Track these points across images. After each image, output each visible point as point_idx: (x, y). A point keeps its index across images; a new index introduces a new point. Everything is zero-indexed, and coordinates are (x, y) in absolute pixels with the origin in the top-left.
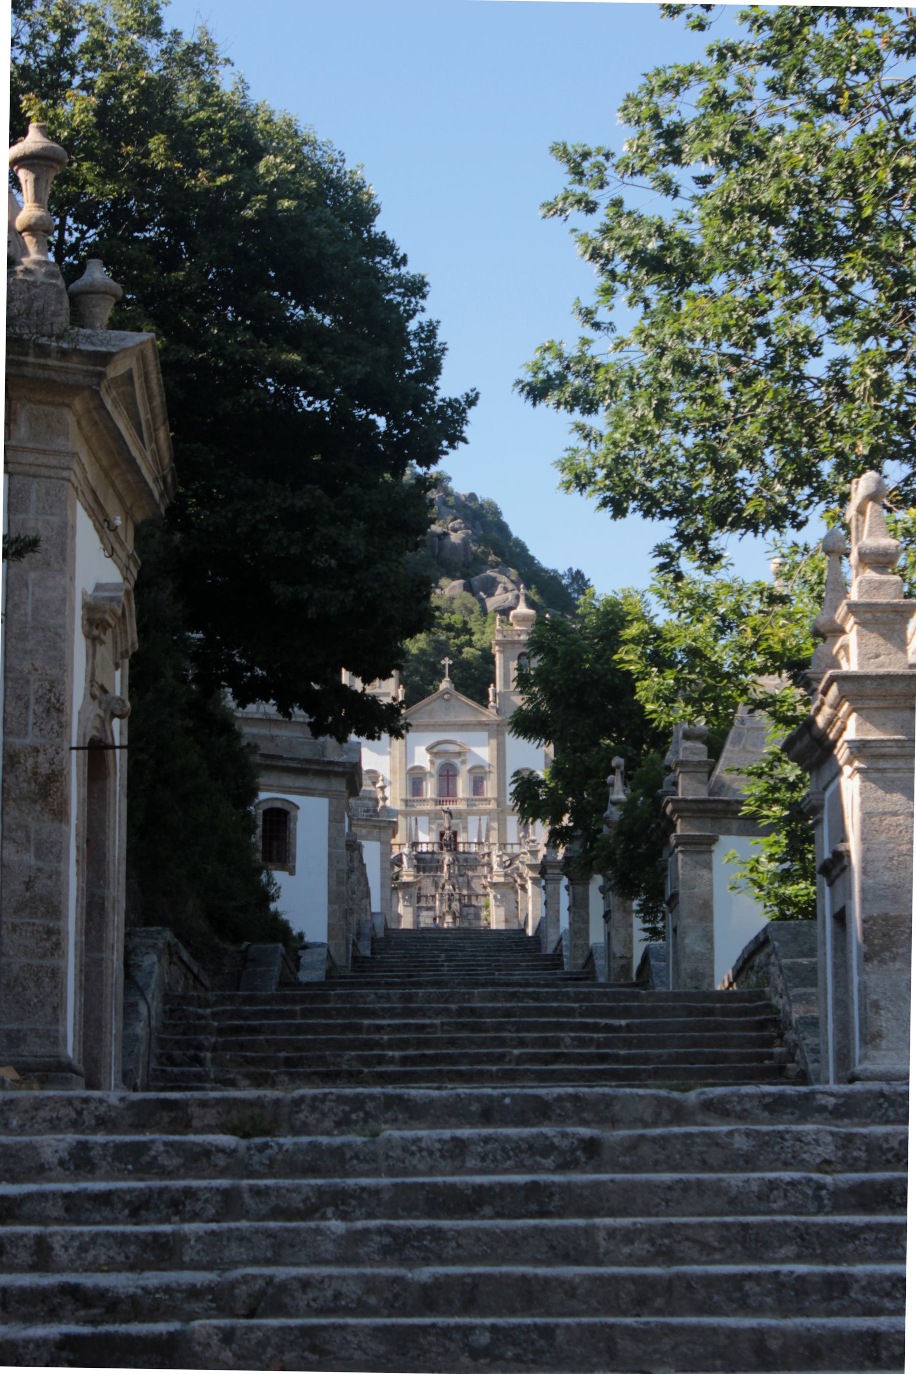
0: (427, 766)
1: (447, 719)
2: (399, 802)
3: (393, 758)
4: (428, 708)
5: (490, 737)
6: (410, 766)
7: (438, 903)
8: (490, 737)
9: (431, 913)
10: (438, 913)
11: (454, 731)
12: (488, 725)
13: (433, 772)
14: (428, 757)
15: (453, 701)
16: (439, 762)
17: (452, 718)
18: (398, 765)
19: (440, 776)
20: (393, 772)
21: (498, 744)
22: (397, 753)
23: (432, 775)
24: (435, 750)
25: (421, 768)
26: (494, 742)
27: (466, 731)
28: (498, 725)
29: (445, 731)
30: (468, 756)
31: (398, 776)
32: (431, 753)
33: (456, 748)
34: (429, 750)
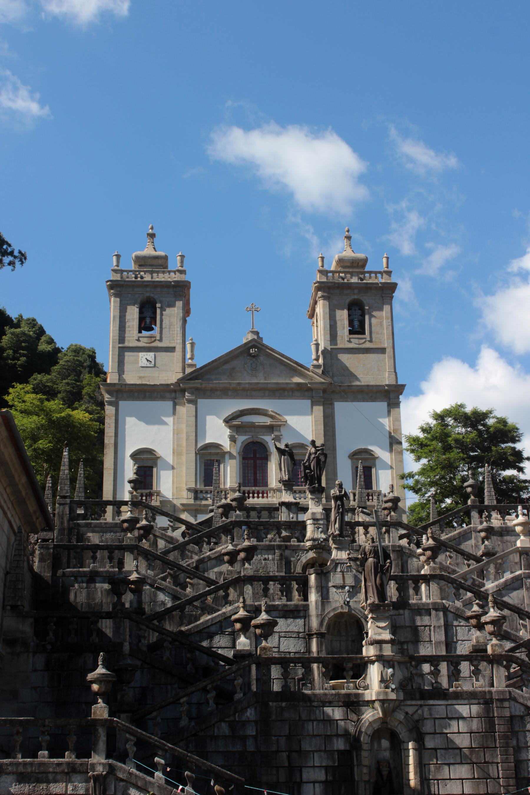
0: (226, 444)
1: (255, 381)
2: (185, 494)
3: (177, 433)
4: (227, 366)
5: (313, 404)
6: (200, 445)
7: (313, 597)
8: (313, 404)
9: (296, 625)
10: (314, 623)
11: (263, 397)
12: (310, 390)
13: (234, 453)
14: (227, 432)
15: (262, 358)
16: (242, 439)
17: (260, 379)
18: (184, 443)
19: (244, 458)
20: (176, 452)
21: (325, 417)
22: (184, 427)
23: (232, 457)
24: (235, 423)
25: (217, 446)
26: (319, 410)
27: (281, 397)
28: (324, 391)
29: (251, 397)
30: (283, 430)
31: (184, 458)
32: (230, 427)
33: (268, 421)
34: (227, 421)
